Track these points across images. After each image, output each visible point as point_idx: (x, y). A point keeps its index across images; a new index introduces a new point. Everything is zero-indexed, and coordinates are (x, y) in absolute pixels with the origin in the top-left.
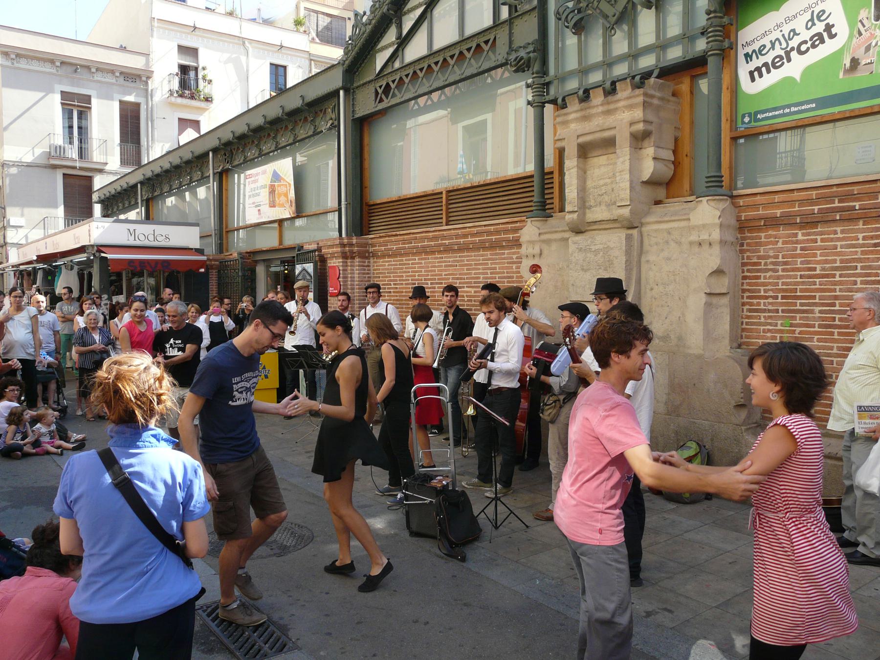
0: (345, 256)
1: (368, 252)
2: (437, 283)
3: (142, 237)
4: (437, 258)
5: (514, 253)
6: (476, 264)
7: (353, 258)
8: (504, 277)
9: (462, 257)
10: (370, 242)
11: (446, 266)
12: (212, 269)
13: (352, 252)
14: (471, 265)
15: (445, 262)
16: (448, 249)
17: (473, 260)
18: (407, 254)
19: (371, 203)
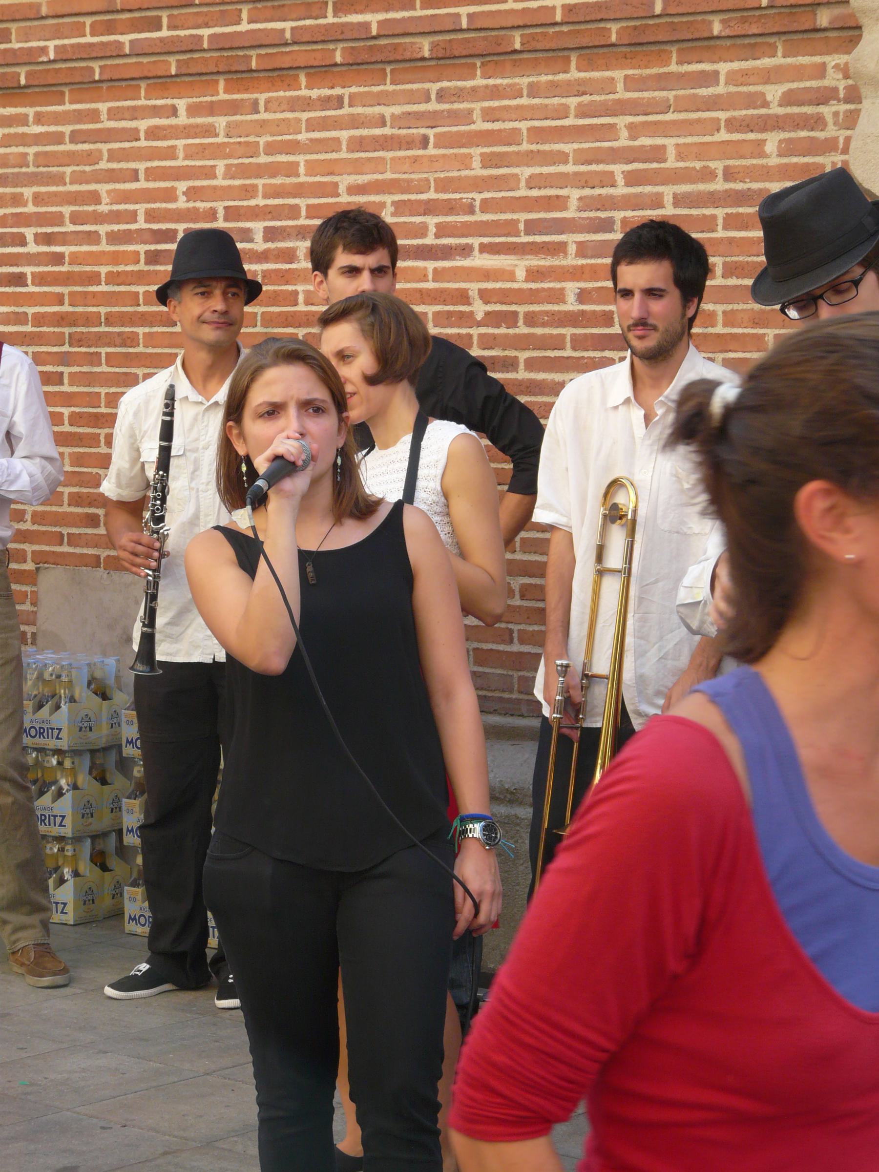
4: (307, 104)
5: (769, 76)
6: (537, 134)
8: (713, 199)
9: (459, 95)
11: (358, 144)
14: (512, 137)
15: (354, 122)
16: (373, 58)
17: (522, 113)
18: (119, 84)
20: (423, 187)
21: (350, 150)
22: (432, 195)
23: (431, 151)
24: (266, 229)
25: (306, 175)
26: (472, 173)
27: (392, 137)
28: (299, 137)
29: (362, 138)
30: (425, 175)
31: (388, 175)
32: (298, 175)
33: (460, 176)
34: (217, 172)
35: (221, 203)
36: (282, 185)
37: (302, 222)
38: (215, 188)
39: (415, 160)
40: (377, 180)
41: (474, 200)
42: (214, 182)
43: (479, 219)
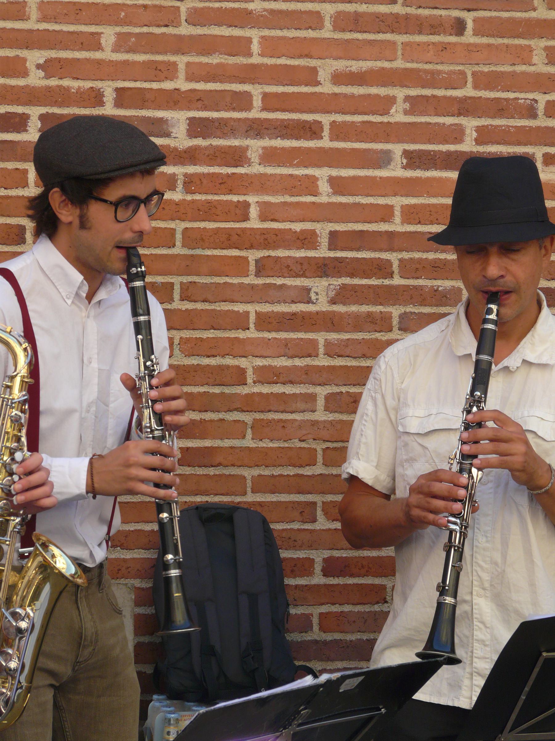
2: (256, 129)
20: (458, 80)
21: (337, 27)
22: (469, 91)
23: (469, 37)
24: (192, 121)
25: (262, 55)
26: (532, 69)
27: (407, 17)
28: (251, 6)
29: (357, 16)
30: (461, 68)
31: (399, 64)
32: (250, 55)
33: (514, 72)
34: (103, 41)
35: (110, 83)
36: (220, 65)
37: (255, 114)
38: (99, 62)
39: (444, 47)
40: (383, 69)
41: (536, 101)
42: (98, 55)
43: (544, 124)
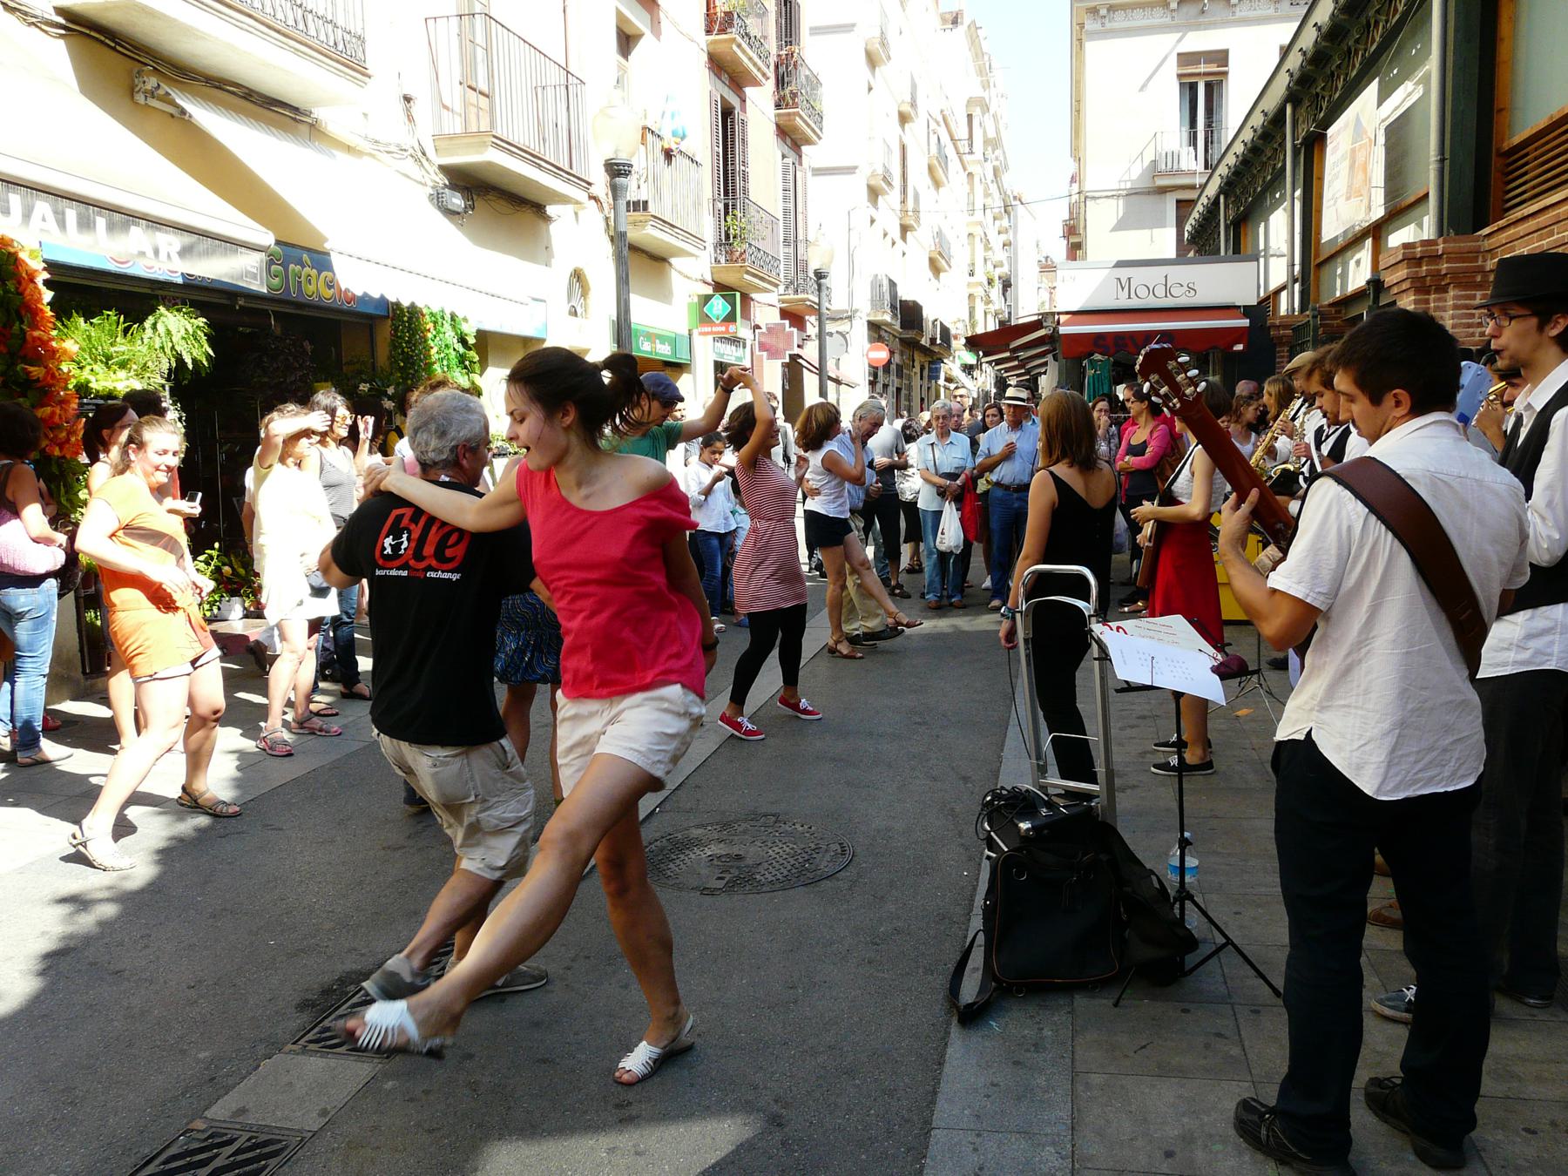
0: (1420, 287)
1: (1481, 270)
3: (1142, 292)
7: (1444, 289)
10: (1487, 245)
12: (1283, 344)
13: (1437, 275)
19: (1506, 146)
